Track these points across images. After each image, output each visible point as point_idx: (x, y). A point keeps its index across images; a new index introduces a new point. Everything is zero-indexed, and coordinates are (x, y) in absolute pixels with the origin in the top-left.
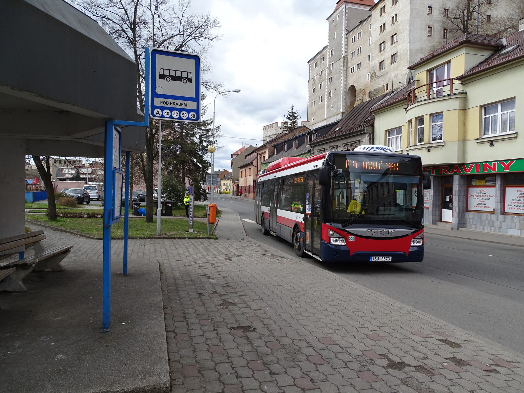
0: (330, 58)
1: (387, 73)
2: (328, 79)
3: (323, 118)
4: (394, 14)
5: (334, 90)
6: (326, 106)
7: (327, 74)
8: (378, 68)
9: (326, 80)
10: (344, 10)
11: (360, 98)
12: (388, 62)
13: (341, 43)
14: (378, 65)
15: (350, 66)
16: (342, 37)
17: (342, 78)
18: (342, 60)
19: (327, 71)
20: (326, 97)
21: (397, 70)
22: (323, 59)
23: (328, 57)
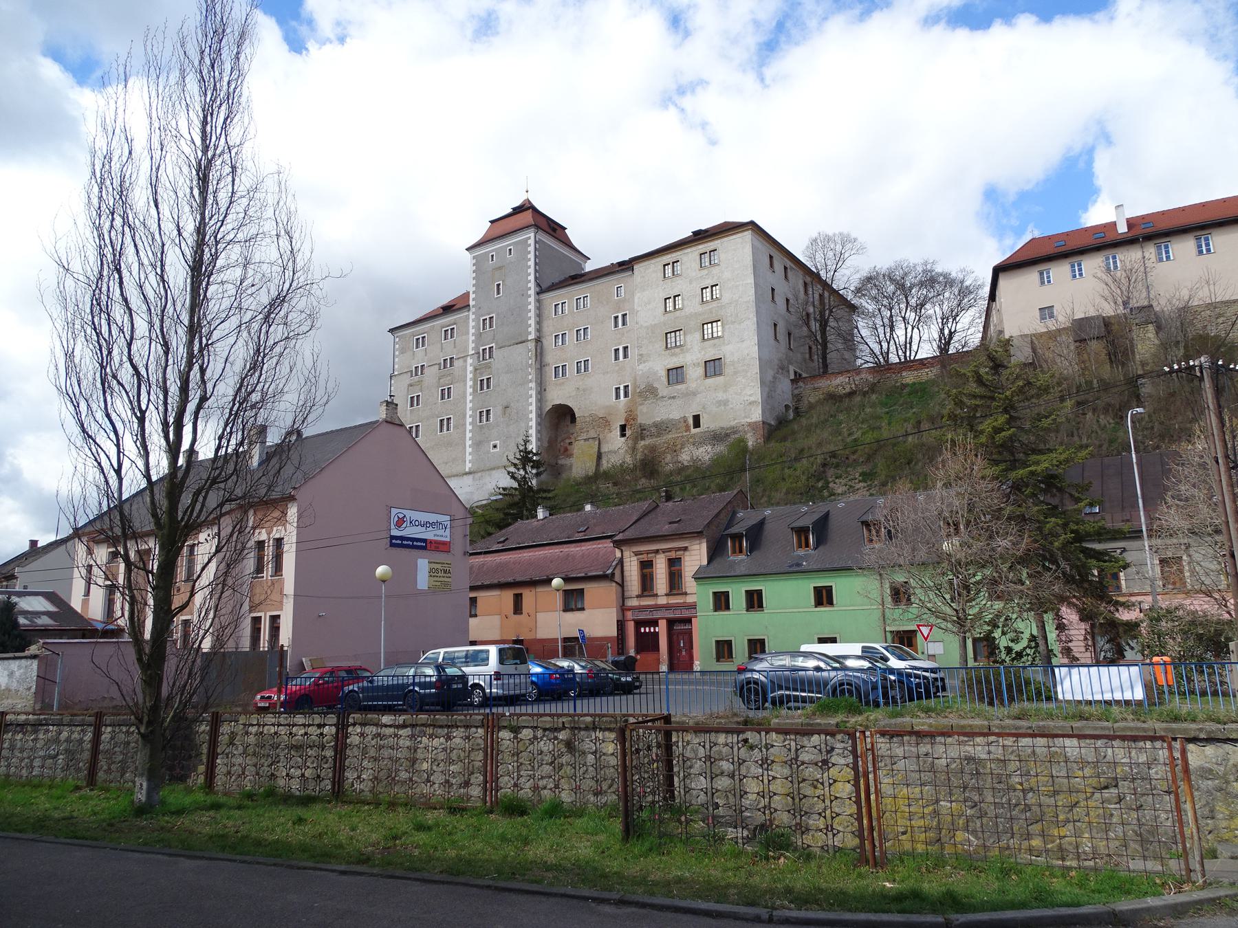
0: (479, 336)
1: (694, 394)
4: (709, 282)
5: (500, 408)
6: (469, 443)
7: (470, 369)
8: (665, 380)
9: (470, 383)
10: (531, 242)
11: (592, 434)
12: (694, 373)
13: (523, 308)
14: (664, 373)
16: (525, 295)
17: (533, 385)
18: (531, 345)
19: (470, 361)
20: (469, 420)
21: (725, 391)
22: (449, 333)
23: (472, 331)
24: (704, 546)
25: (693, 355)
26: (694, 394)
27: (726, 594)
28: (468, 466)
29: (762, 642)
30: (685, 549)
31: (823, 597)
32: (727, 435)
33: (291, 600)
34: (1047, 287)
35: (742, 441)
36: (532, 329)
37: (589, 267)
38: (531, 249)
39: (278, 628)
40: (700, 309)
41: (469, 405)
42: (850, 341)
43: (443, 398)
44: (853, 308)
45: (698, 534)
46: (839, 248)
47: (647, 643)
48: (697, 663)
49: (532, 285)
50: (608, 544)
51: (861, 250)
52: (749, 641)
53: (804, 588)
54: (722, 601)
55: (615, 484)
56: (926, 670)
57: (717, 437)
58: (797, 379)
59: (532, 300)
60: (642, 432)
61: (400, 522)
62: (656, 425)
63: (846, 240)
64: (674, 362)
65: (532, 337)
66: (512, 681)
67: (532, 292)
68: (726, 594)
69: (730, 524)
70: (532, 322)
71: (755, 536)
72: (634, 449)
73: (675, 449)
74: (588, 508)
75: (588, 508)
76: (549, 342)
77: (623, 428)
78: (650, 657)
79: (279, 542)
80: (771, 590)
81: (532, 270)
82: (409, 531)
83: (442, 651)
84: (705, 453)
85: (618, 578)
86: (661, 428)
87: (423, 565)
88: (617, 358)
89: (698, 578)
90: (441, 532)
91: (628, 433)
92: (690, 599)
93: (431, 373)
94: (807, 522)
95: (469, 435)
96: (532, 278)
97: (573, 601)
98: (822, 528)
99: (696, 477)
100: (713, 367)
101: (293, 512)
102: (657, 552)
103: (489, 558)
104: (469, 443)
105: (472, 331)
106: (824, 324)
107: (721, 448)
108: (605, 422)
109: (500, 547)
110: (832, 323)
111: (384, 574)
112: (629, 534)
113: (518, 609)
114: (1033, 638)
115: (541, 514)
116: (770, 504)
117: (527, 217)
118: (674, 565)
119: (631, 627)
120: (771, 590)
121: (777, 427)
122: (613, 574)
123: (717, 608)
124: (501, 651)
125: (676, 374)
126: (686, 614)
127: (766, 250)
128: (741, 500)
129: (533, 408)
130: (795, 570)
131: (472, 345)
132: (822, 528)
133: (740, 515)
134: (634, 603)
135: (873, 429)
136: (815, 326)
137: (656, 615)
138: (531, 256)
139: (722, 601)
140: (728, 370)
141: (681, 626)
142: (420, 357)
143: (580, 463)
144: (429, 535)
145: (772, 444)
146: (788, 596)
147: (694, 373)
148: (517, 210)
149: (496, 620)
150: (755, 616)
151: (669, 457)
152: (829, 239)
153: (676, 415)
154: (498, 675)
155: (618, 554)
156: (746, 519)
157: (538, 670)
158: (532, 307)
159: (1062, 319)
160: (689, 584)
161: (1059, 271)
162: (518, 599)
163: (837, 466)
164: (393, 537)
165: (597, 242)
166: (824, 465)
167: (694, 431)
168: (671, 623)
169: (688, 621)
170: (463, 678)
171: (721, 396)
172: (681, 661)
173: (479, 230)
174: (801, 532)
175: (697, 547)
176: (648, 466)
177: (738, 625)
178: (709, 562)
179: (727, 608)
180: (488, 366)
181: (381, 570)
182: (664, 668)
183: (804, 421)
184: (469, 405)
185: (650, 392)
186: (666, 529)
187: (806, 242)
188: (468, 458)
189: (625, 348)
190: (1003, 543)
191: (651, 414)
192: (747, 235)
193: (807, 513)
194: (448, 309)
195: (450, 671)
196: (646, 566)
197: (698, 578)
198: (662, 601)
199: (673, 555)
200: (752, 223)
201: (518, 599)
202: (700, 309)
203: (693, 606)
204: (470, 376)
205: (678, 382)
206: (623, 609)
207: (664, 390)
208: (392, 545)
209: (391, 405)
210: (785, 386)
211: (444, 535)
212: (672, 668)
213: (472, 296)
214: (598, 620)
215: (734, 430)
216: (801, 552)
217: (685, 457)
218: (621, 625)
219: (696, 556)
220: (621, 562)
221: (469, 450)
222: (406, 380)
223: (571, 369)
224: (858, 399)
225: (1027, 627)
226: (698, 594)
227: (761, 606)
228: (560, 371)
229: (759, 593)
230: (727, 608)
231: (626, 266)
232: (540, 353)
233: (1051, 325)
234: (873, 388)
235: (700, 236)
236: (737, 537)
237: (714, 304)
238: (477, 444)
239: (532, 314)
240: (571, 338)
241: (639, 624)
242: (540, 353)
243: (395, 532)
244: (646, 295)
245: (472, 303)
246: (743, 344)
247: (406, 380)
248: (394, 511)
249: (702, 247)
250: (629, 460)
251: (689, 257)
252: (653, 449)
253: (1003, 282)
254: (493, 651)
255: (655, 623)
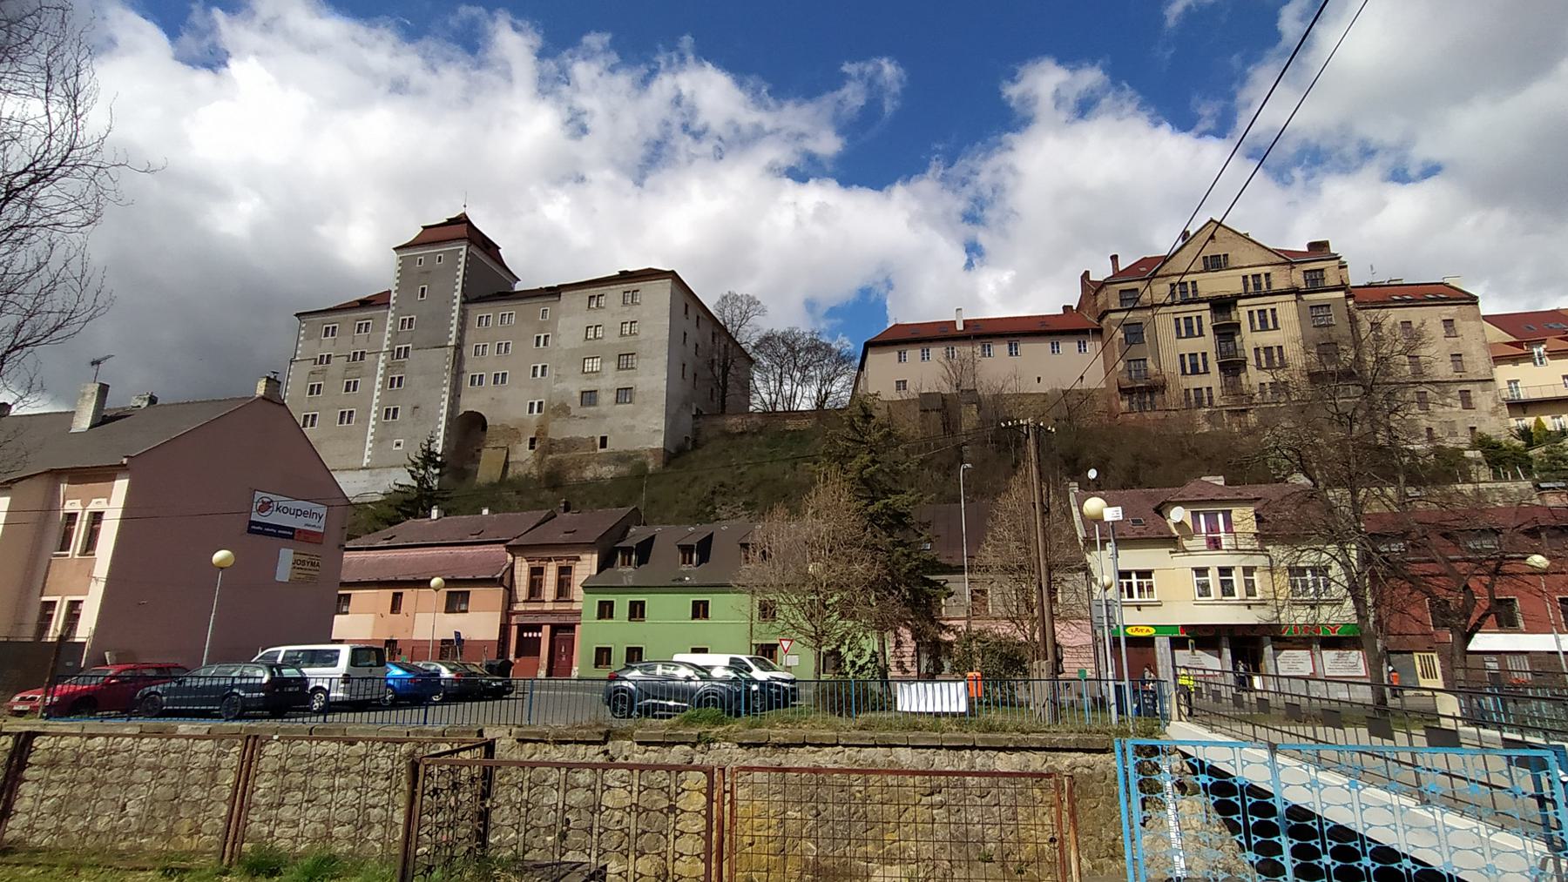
0: (395, 334)
1: (604, 417)
2: (385, 376)
3: (356, 464)
4: (630, 318)
7: (381, 365)
9: (379, 379)
10: (463, 253)
14: (578, 395)
15: (470, 368)
17: (447, 389)
18: (450, 352)
19: (382, 357)
24: (596, 556)
25: (609, 381)
26: (604, 417)
27: (611, 604)
28: (366, 461)
29: (640, 650)
30: (578, 559)
31: (700, 610)
32: (630, 458)
33: (102, 585)
34: (903, 364)
35: (644, 464)
36: (453, 336)
37: (518, 287)
38: (462, 260)
39: (78, 616)
40: (618, 340)
41: (376, 401)
42: (746, 390)
43: (347, 390)
44: (752, 361)
45: (588, 547)
46: (744, 307)
47: (528, 648)
48: (575, 668)
49: (458, 294)
50: (501, 548)
51: (763, 311)
52: (628, 649)
53: (686, 601)
54: (606, 610)
55: (518, 493)
56: (784, 681)
57: (621, 458)
58: (698, 414)
59: (457, 308)
60: (551, 447)
61: (266, 506)
62: (564, 441)
63: (752, 301)
64: (588, 385)
65: (452, 343)
66: (362, 684)
67: (457, 301)
68: (611, 604)
69: (623, 536)
70: (454, 329)
71: (644, 551)
72: (540, 461)
73: (580, 467)
74: (485, 512)
75: (485, 512)
76: (468, 352)
77: (533, 441)
78: (528, 660)
79: (97, 517)
80: (651, 601)
81: (460, 280)
82: (274, 518)
83: (283, 649)
84: (607, 472)
85: (506, 582)
86: (570, 444)
87: (287, 556)
88: (534, 375)
89: (588, 588)
90: (313, 521)
91: (537, 446)
92: (576, 607)
93: (337, 365)
94: (694, 541)
95: (371, 430)
96: (459, 287)
97: (456, 602)
98: (704, 549)
99: (598, 493)
100: (624, 394)
101: (121, 486)
102: (549, 560)
103: (372, 554)
104: (370, 438)
105: (388, 328)
106: (726, 370)
107: (624, 470)
108: (514, 433)
109: (385, 543)
110: (732, 370)
111: (225, 559)
112: (523, 541)
113: (396, 606)
114: (874, 654)
115: (435, 513)
116: (661, 523)
117: (462, 230)
118: (565, 572)
119: (514, 630)
120: (651, 601)
121: (676, 454)
122: (502, 578)
123: (601, 616)
124: (354, 652)
125: (589, 397)
126: (570, 620)
127: (682, 298)
128: (635, 518)
129: (444, 411)
130: (677, 587)
131: (387, 342)
132: (704, 549)
133: (632, 530)
134: (519, 607)
135: (757, 464)
136: (718, 371)
137: (541, 620)
138: (461, 267)
139: (606, 610)
140: (636, 399)
141: (564, 631)
142: (327, 346)
143: (487, 470)
144: (298, 523)
145: (670, 470)
146: (667, 608)
147: (606, 398)
148: (451, 222)
149: (369, 619)
150: (636, 625)
151: (573, 473)
152: (736, 298)
153: (584, 434)
154: (347, 678)
155: (510, 558)
156: (637, 534)
157: (398, 672)
158: (455, 315)
159: (912, 391)
160: (577, 592)
161: (913, 353)
162: (397, 599)
163: (724, 494)
164: (252, 523)
165: (528, 264)
166: (713, 493)
167: (600, 451)
168: (555, 628)
169: (571, 627)
170: (303, 681)
171: (628, 421)
172: (559, 665)
173: (412, 233)
174: (686, 550)
175: (587, 556)
176: (553, 479)
177: (619, 633)
178: (599, 571)
179: (611, 617)
180: (402, 365)
181: (220, 556)
182: (542, 673)
183: (700, 452)
184: (376, 401)
185: (563, 410)
186: (561, 538)
187: (718, 298)
188: (368, 452)
189: (544, 367)
190: (858, 567)
191: (561, 430)
192: (668, 282)
193: (693, 533)
194: (365, 303)
195: (288, 672)
196: (536, 572)
197: (588, 588)
198: (548, 607)
199: (564, 563)
200: (673, 272)
201: (397, 599)
202: (618, 340)
203: (578, 613)
204: (380, 372)
205: (590, 404)
206: (507, 613)
207: (576, 409)
208: (250, 531)
209: (273, 383)
210: (687, 420)
211: (318, 526)
212: (549, 673)
213: (393, 295)
214: (480, 623)
215: (637, 454)
216: (685, 568)
217: (588, 474)
218: (505, 629)
219: (587, 565)
220: (512, 567)
221: (369, 445)
222: (310, 366)
223: (488, 380)
224: (747, 438)
225: (871, 644)
226: (583, 601)
227: (642, 615)
228: (477, 380)
229: (642, 604)
230: (611, 617)
231: (555, 292)
232: (458, 361)
233: (904, 395)
234: (761, 431)
235: (626, 276)
236: (627, 551)
237: (632, 338)
238: (379, 441)
239: (455, 322)
240: (491, 350)
241: (522, 628)
242: (458, 361)
243: (255, 517)
244: (570, 321)
245: (392, 301)
246: (653, 378)
247: (310, 366)
248: (258, 495)
249: (626, 287)
250: (534, 471)
251: (614, 293)
252: (559, 463)
253: (872, 357)
254: (345, 652)
255: (538, 628)
